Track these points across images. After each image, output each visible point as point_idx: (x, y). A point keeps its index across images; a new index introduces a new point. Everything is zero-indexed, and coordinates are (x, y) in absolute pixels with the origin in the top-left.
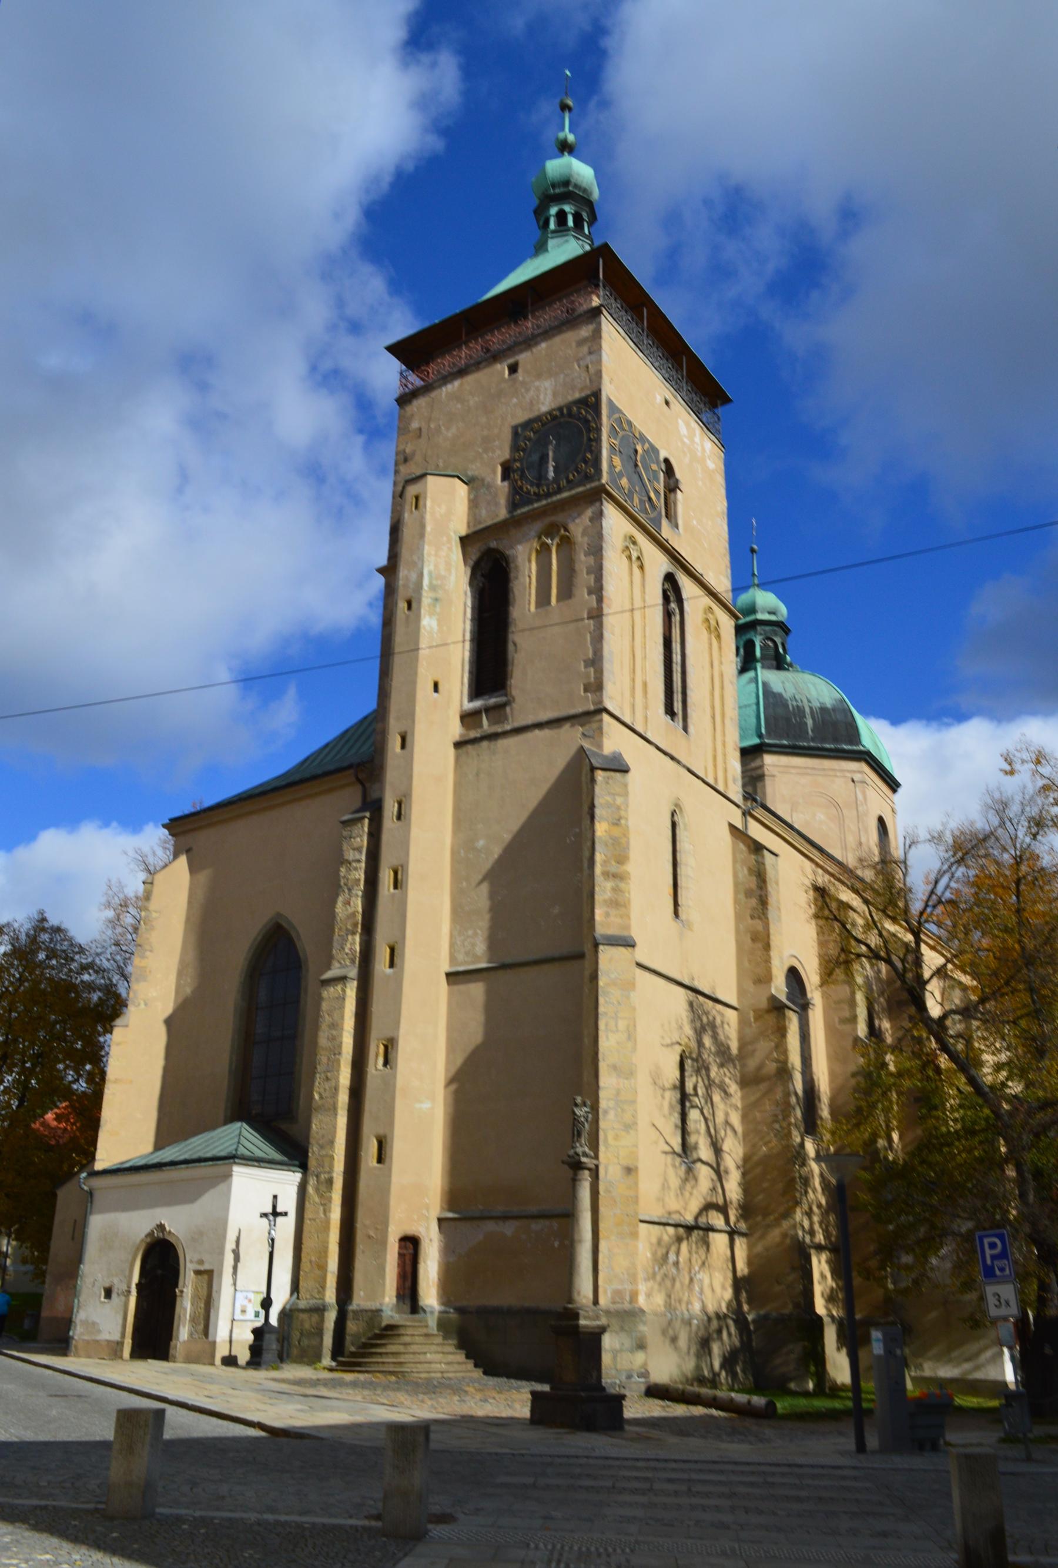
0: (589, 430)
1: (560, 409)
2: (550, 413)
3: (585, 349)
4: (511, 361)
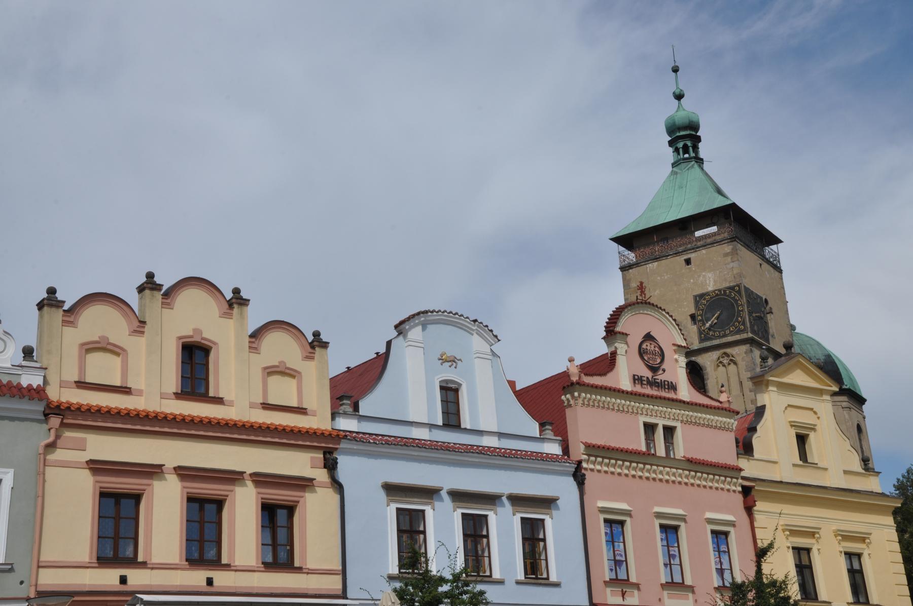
0: (738, 306)
1: (720, 290)
2: (714, 291)
3: (729, 259)
4: (686, 257)
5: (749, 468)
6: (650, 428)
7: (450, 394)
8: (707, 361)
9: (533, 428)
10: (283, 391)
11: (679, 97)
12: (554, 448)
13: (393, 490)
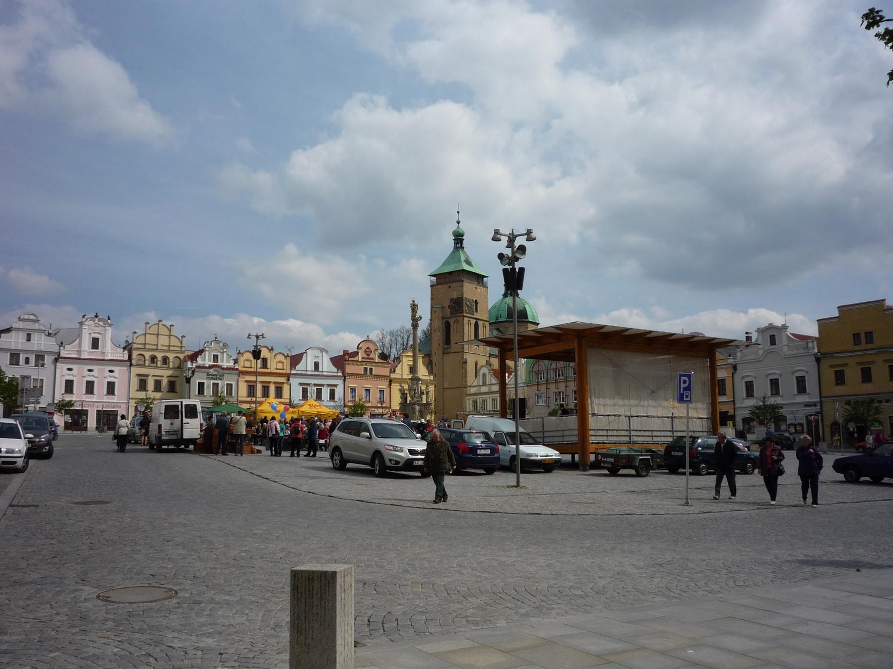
5: (393, 376)
6: (365, 369)
7: (316, 365)
8: (452, 321)
9: (335, 370)
10: (280, 366)
11: (458, 222)
12: (340, 374)
13: (301, 384)
